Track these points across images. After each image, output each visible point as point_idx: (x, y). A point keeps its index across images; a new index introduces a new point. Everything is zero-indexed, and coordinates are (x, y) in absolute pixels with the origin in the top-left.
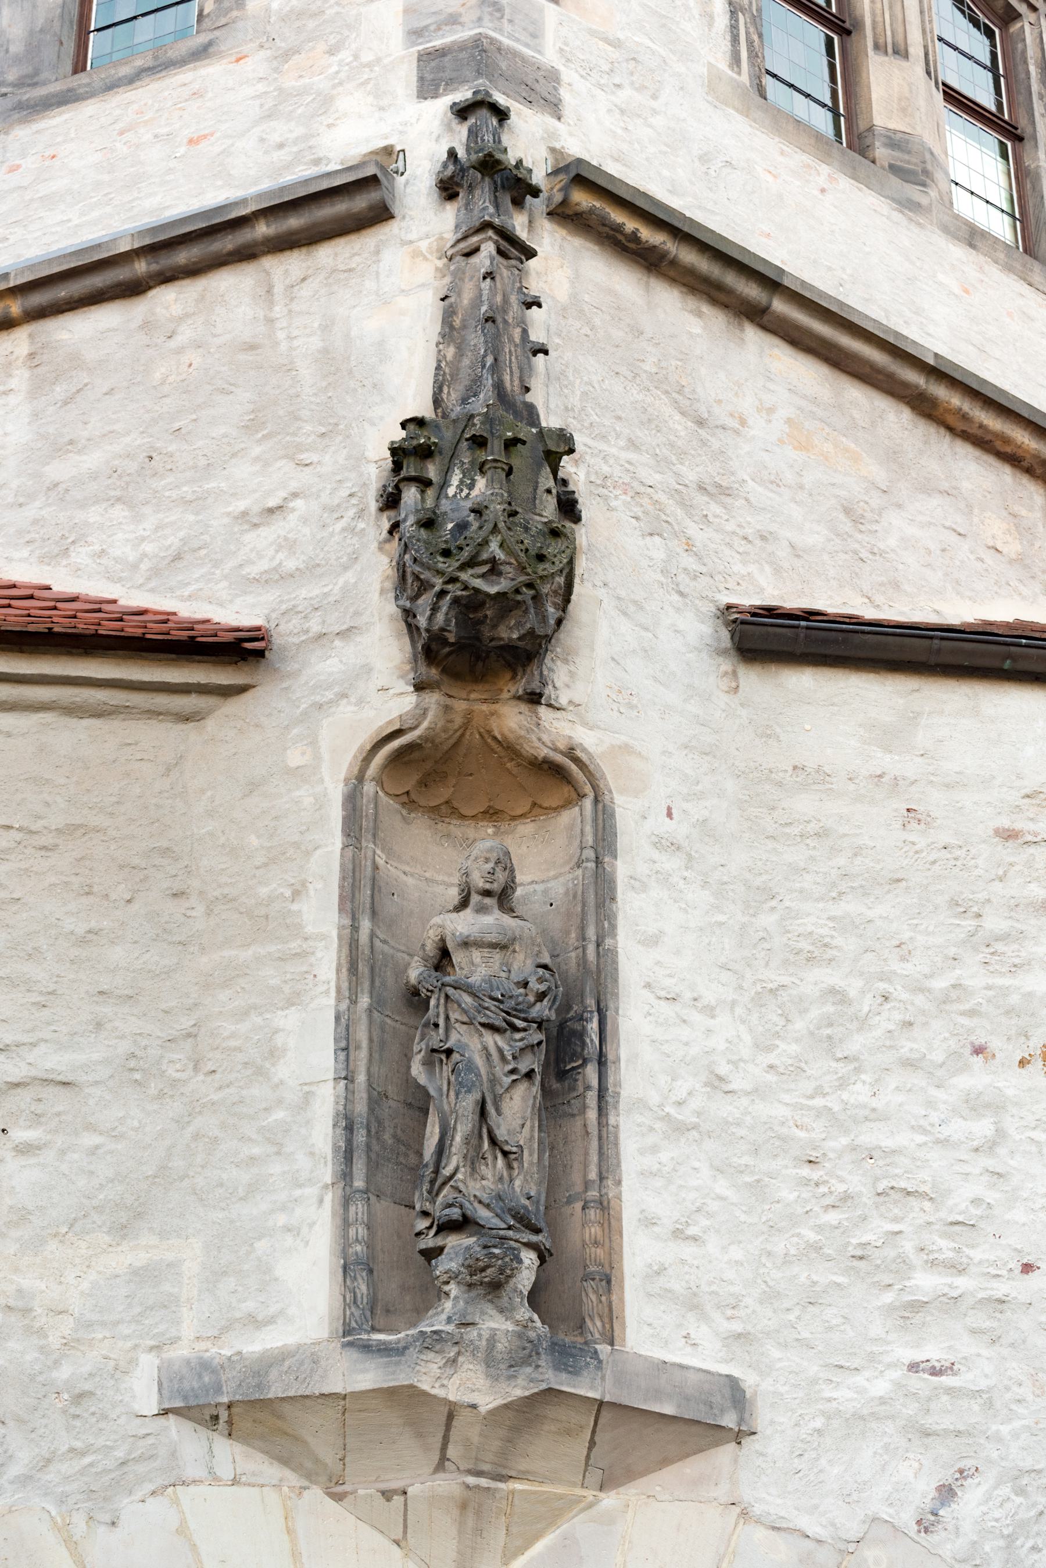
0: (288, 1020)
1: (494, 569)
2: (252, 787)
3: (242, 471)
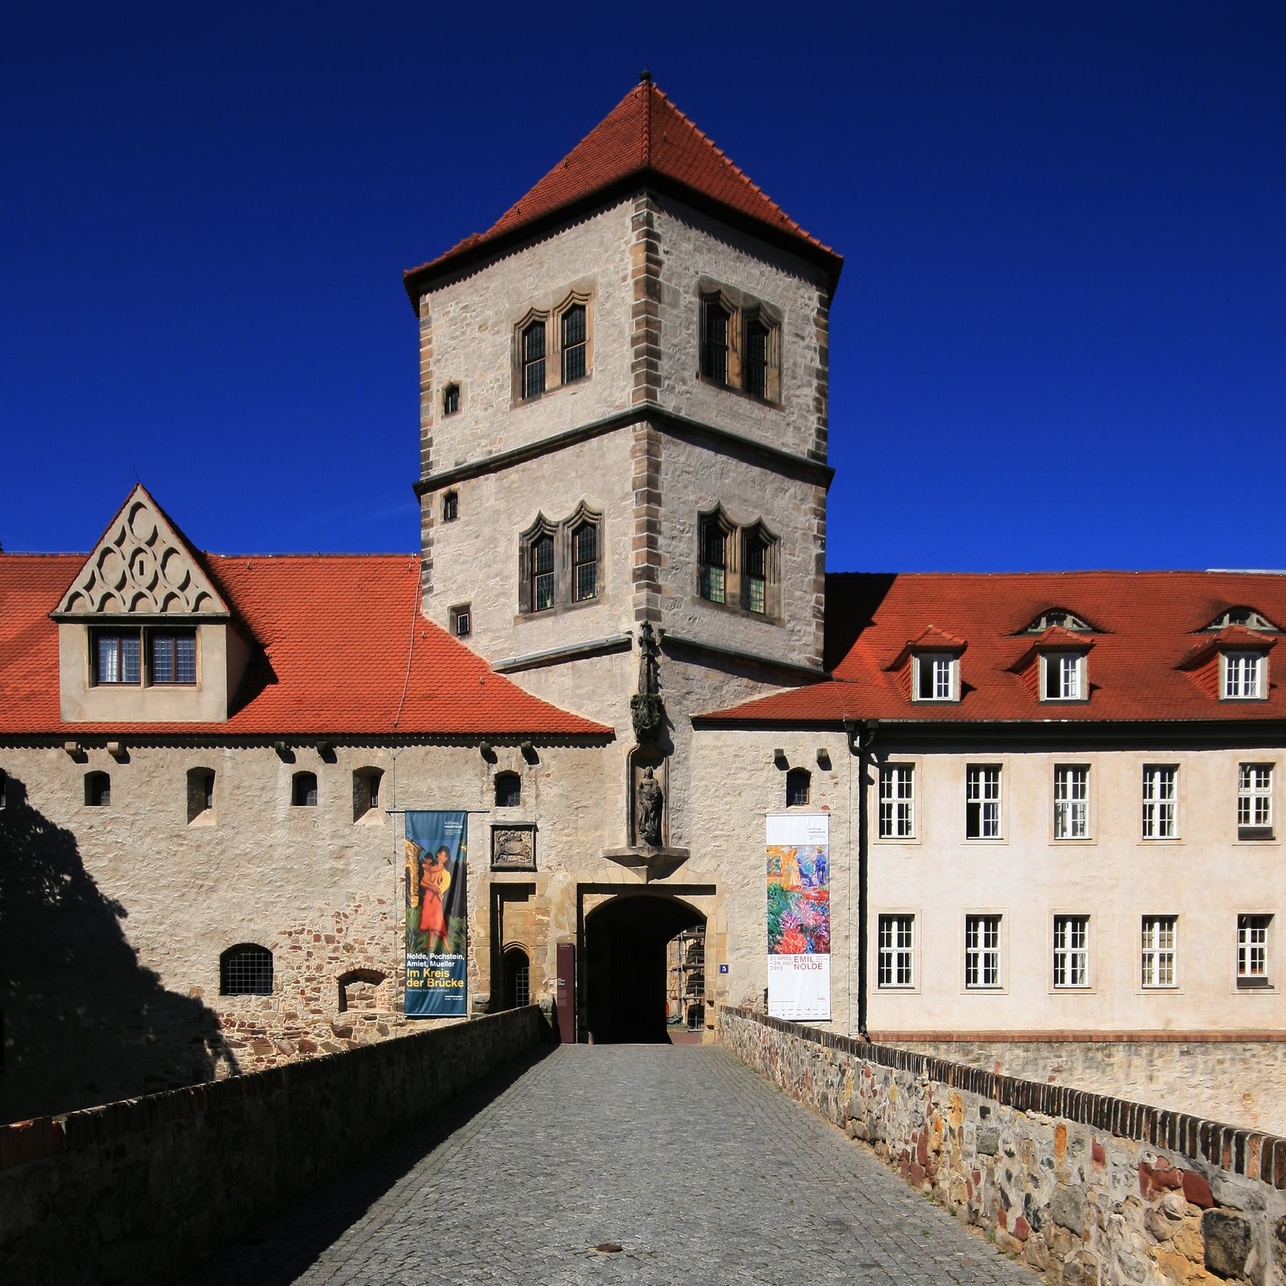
0: (619, 796)
1: (647, 725)
2: (612, 756)
3: (609, 696)
